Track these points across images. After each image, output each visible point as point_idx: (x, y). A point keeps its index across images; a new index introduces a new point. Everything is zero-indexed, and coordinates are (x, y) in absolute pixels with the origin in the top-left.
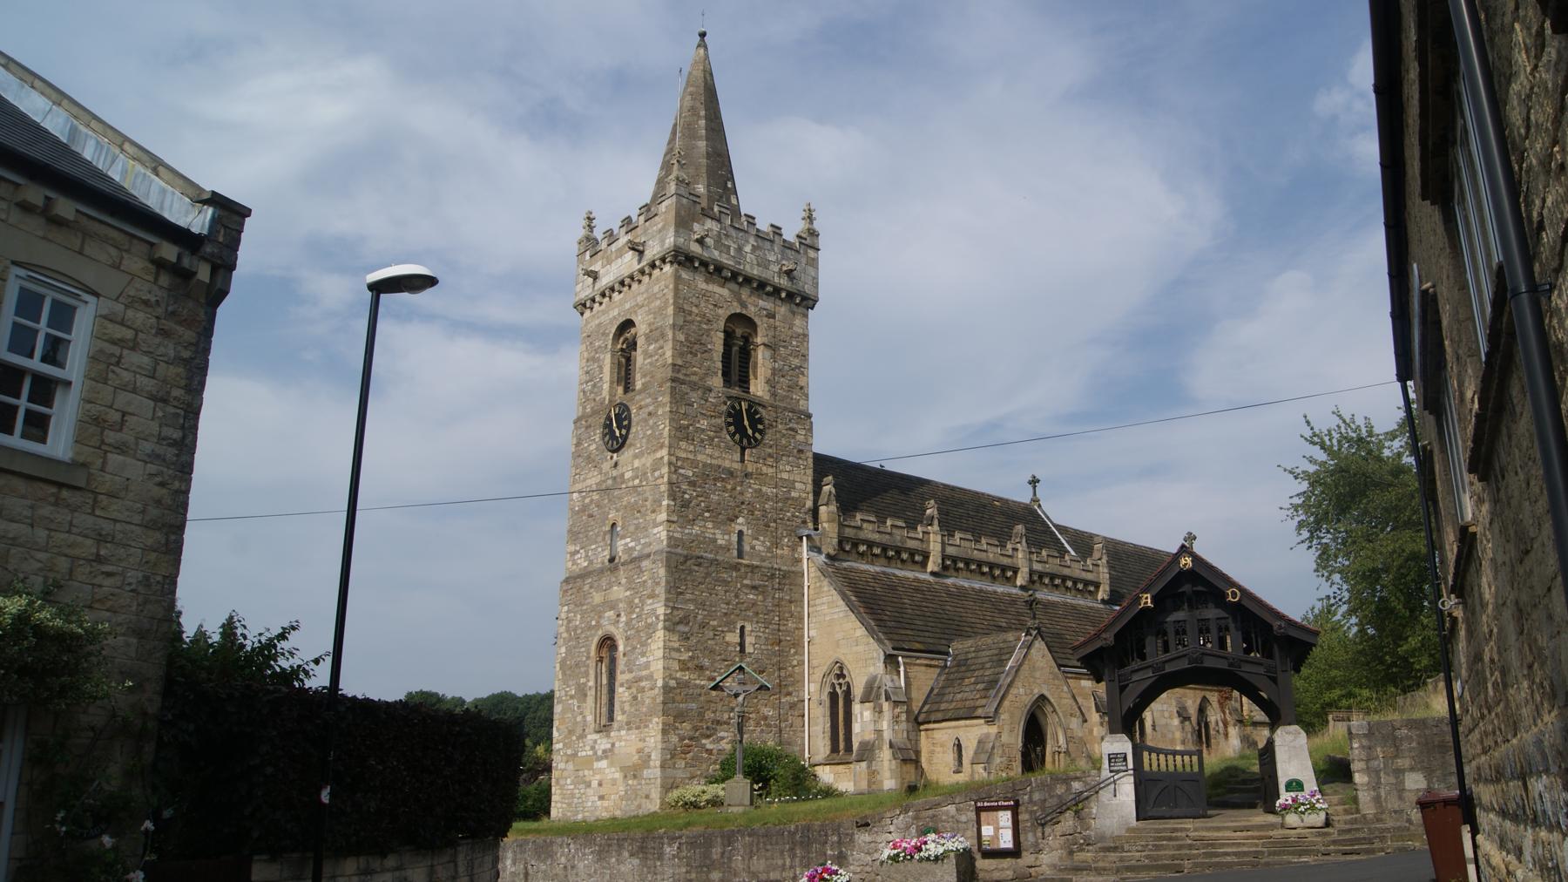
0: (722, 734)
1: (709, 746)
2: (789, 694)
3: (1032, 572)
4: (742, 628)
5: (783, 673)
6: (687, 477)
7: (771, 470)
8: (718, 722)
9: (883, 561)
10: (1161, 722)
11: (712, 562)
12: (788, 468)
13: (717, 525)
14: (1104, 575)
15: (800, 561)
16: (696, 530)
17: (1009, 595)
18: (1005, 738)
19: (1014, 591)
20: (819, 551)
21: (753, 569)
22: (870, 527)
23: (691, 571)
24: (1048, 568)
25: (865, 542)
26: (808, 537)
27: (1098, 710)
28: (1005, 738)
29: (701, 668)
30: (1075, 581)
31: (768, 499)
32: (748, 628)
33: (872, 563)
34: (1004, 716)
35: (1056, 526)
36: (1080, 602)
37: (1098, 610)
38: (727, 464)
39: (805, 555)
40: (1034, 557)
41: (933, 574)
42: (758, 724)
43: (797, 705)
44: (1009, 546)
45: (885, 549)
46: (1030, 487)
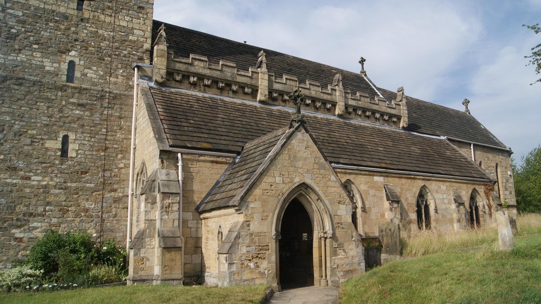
0: (35, 224)
1: (18, 235)
2: (115, 190)
3: (347, 106)
4: (66, 138)
5: (107, 174)
6: (16, 16)
7: (108, 19)
8: (31, 215)
9: (215, 90)
10: (441, 207)
11: (34, 83)
12: (127, 18)
13: (45, 55)
14: (404, 111)
15: (132, 87)
16: (22, 57)
17: (327, 120)
18: (254, 227)
19: (332, 118)
20: (150, 79)
21: (81, 90)
22: (202, 64)
23: (9, 89)
24: (360, 104)
25: (195, 74)
26: (139, 67)
27: (388, 199)
28: (254, 227)
29: (14, 169)
30: (382, 114)
31: (104, 39)
32: (72, 136)
33: (205, 91)
34: (254, 204)
35: (379, 89)
36: (387, 127)
37: (399, 133)
38: (62, 10)
39: (136, 83)
40: (349, 96)
41: (261, 102)
42: (76, 216)
43: (120, 200)
44: (329, 87)
45: (215, 81)
46: (360, 65)
